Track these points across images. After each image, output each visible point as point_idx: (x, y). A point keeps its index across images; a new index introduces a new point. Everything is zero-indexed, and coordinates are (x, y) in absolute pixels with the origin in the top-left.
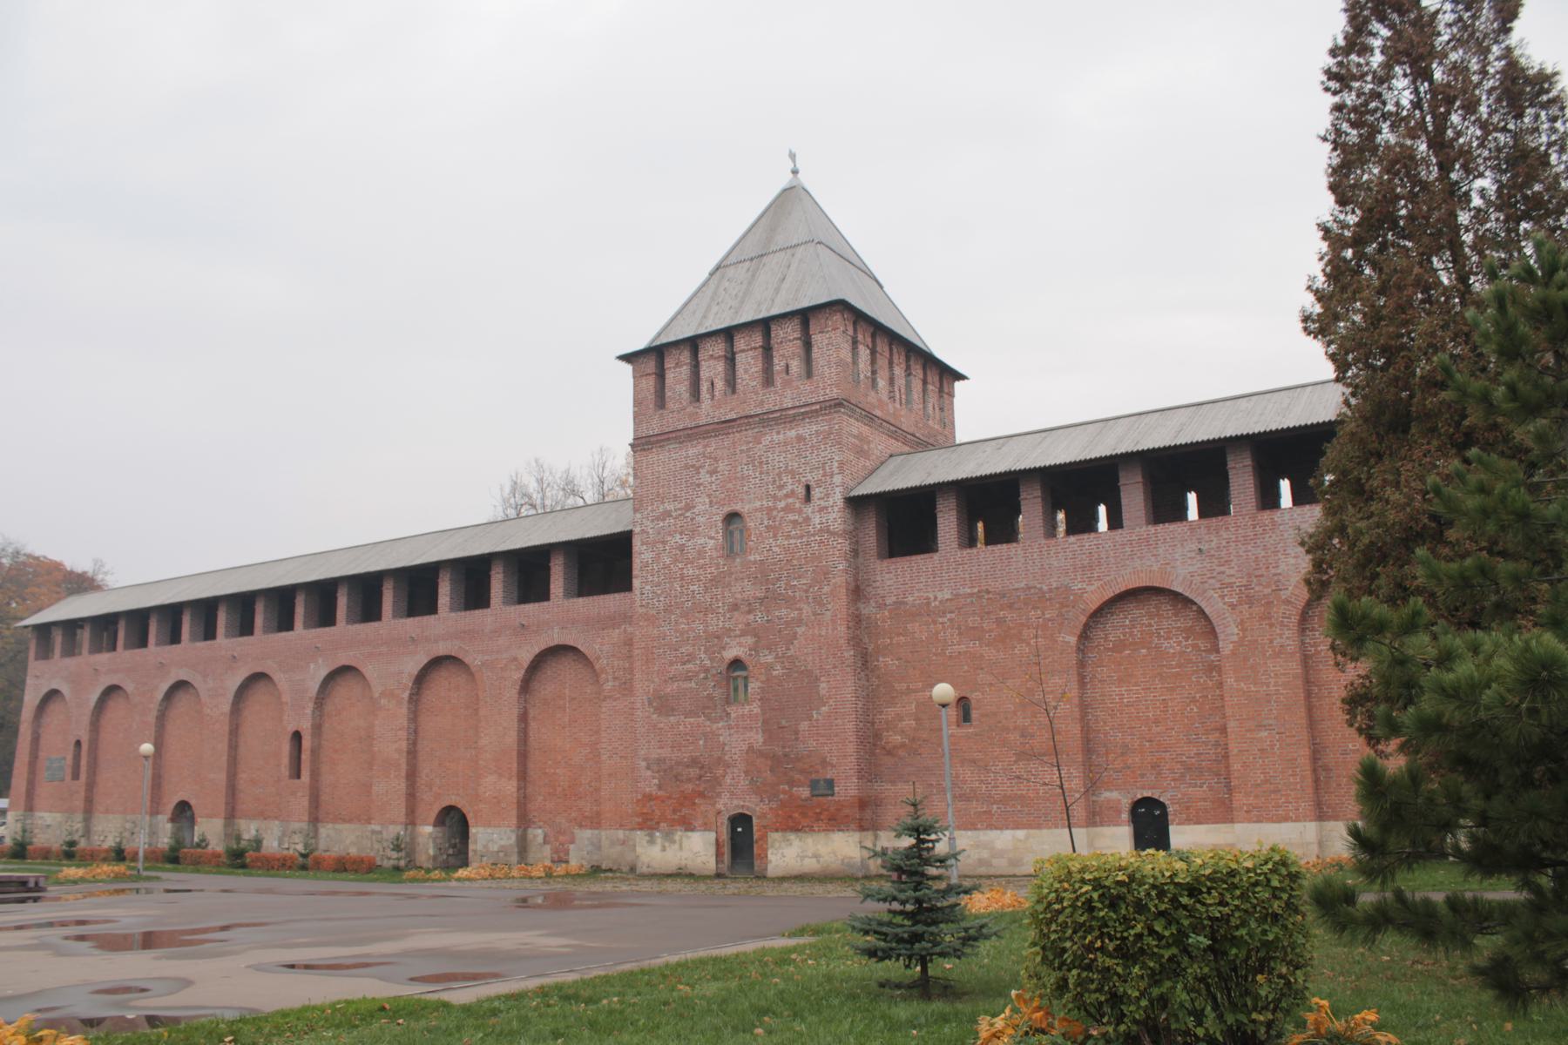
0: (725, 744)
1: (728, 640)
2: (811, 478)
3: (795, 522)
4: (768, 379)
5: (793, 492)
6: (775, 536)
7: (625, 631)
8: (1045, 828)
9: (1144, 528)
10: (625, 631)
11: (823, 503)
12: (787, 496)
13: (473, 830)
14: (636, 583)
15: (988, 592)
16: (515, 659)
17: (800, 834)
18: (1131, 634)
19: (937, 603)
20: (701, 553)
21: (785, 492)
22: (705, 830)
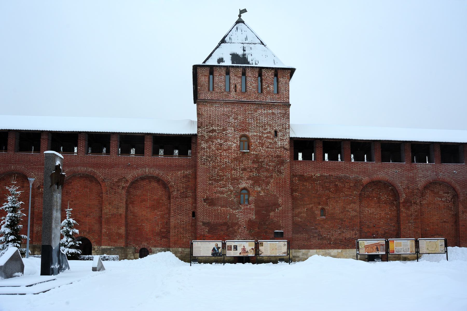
0: (239, 218)
1: (241, 181)
3: (271, 143)
5: (270, 132)
8: (347, 249)
10: (184, 172)
11: (282, 138)
12: (267, 133)
21: (267, 131)
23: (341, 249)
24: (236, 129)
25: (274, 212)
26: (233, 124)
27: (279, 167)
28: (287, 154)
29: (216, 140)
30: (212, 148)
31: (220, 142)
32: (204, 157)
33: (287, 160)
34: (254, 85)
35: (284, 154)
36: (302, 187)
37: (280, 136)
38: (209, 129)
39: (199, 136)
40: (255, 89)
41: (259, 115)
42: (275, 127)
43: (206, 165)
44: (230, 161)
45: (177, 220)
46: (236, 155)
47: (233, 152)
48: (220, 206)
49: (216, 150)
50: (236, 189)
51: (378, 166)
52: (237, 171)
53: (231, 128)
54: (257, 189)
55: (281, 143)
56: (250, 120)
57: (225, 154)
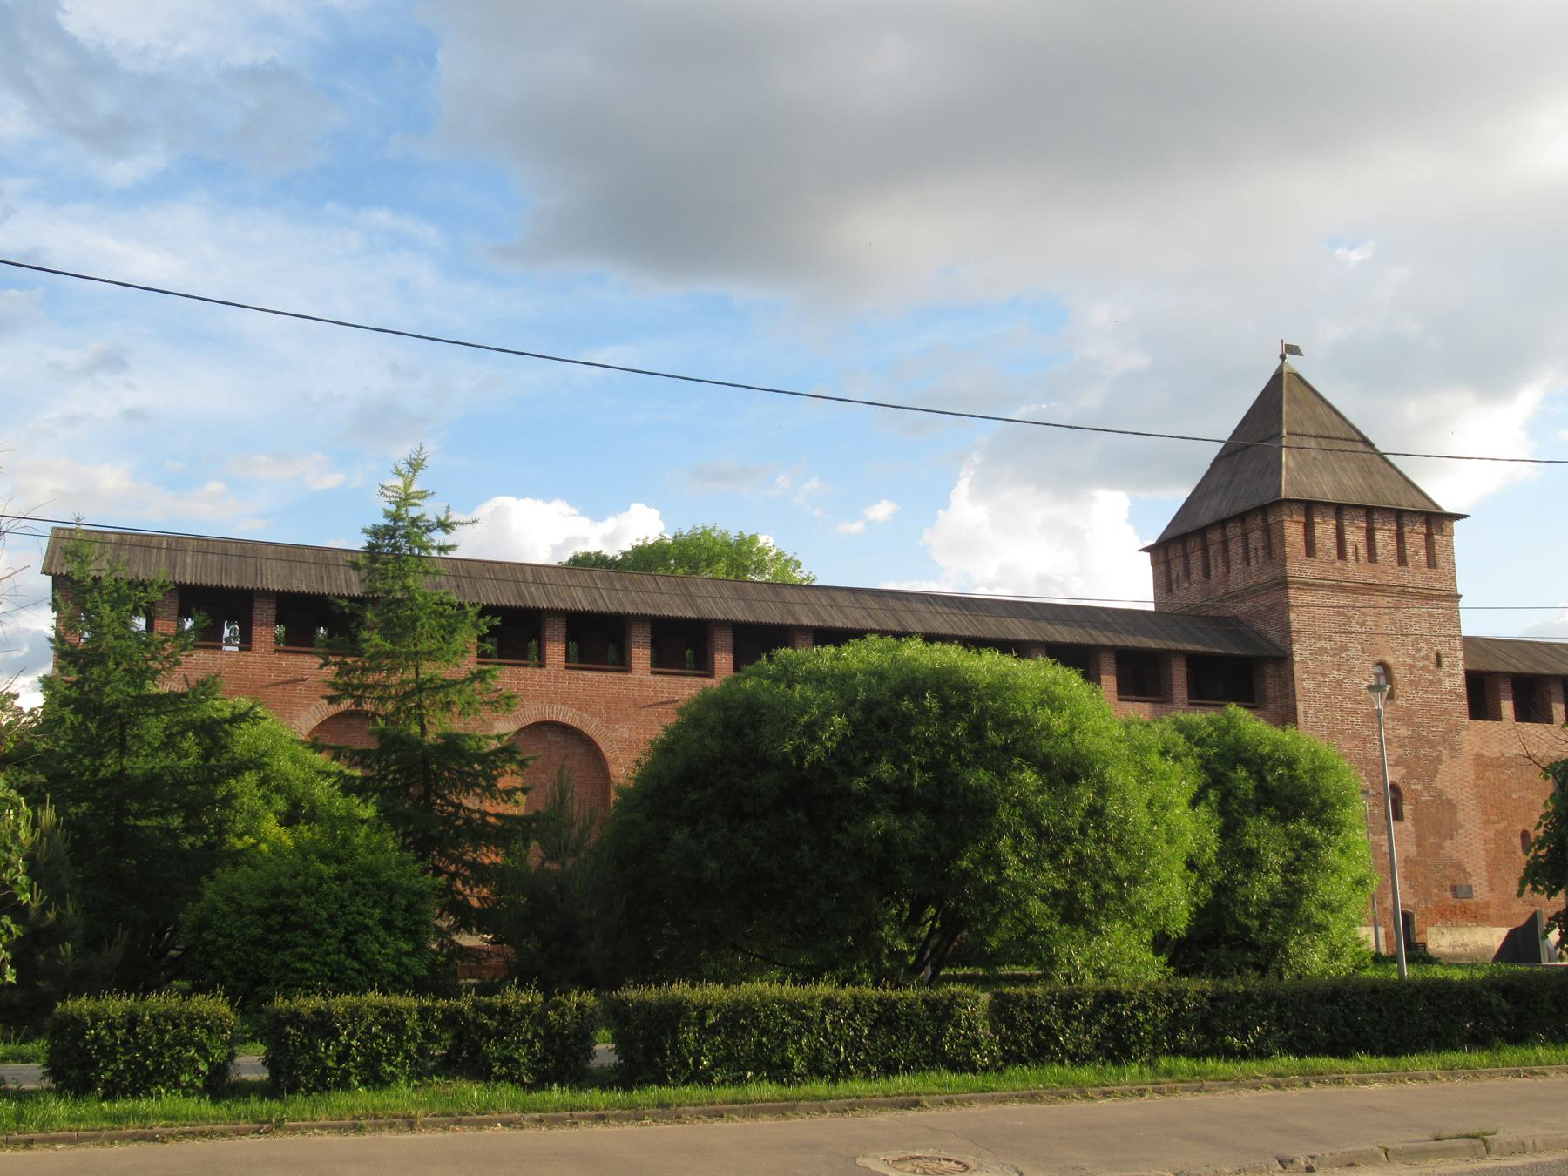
3: (1431, 682)
5: (1427, 655)
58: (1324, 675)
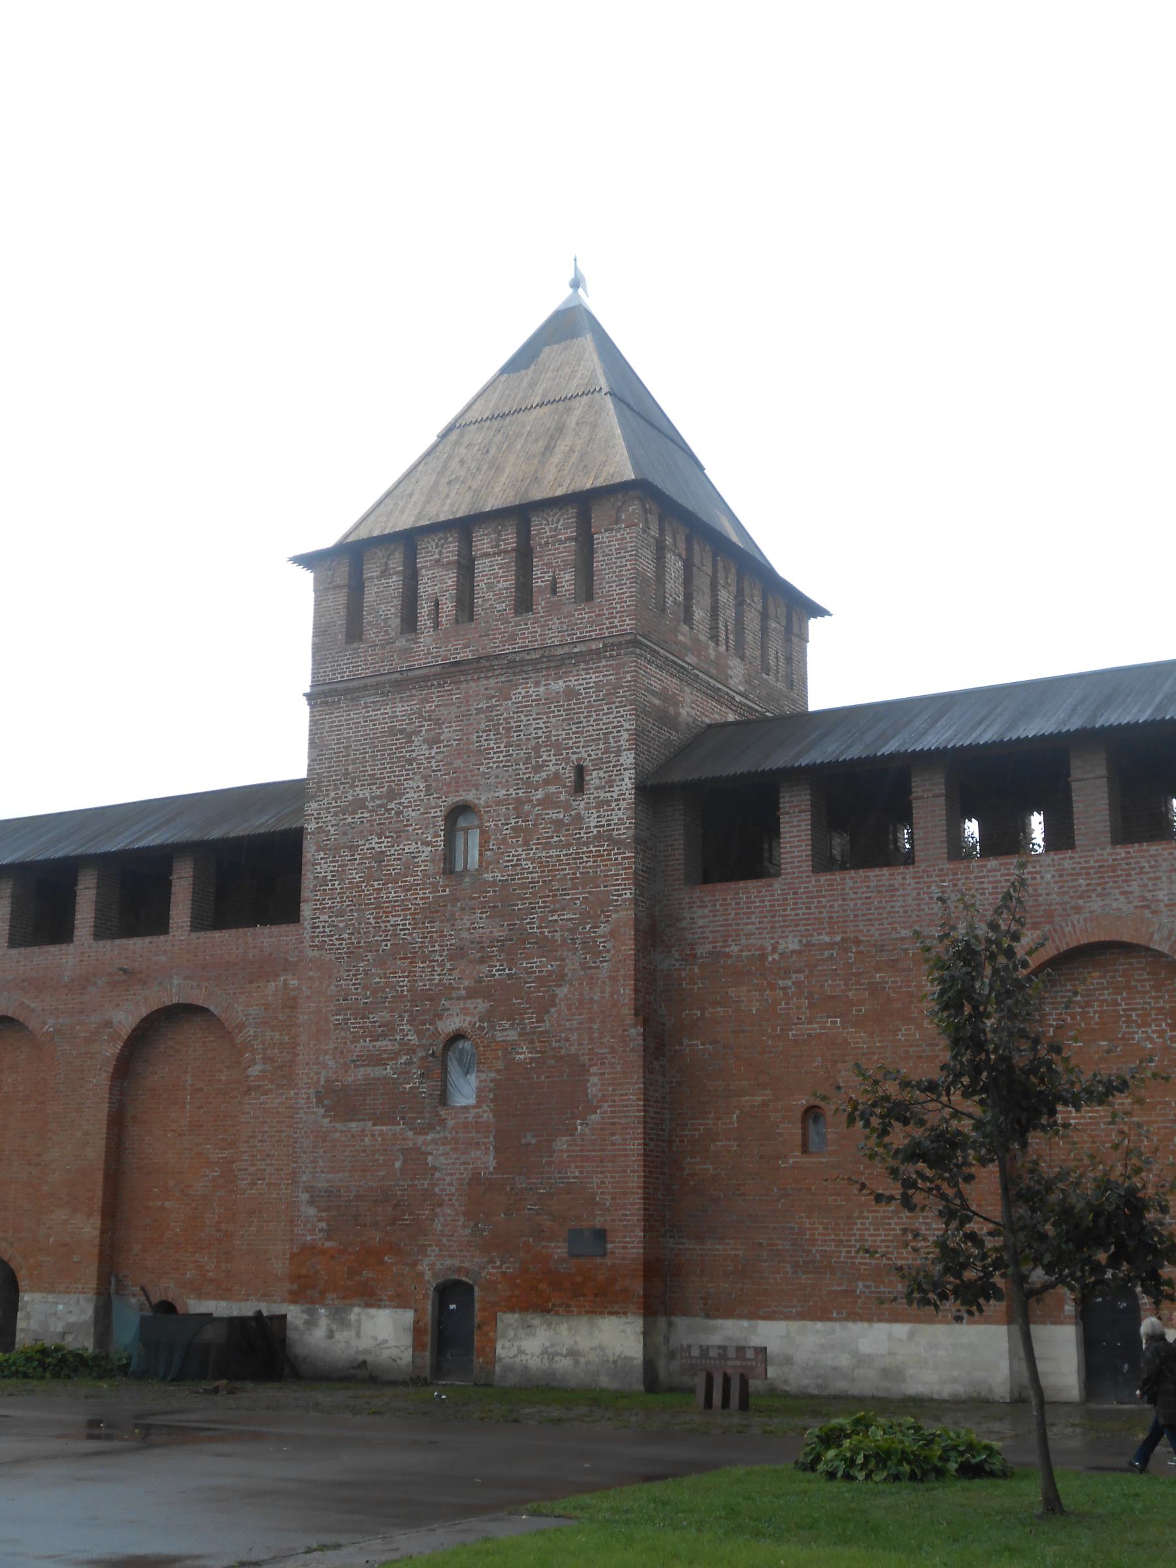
0: (435, 1168)
1: (447, 1004)
2: (586, 755)
3: (558, 823)
4: (524, 600)
5: (556, 774)
6: (526, 843)
7: (285, 983)
9: (1109, 850)
10: (285, 983)
11: (602, 794)
12: (547, 782)
13: (26, 1297)
14: (306, 910)
15: (858, 942)
16: (109, 1024)
17: (548, 1316)
18: (1084, 1014)
19: (776, 957)
20: (409, 866)
21: (544, 775)
22: (397, 1307)
23: (909, 1321)
24: (434, 785)
25: (571, 1135)
26: (422, 764)
27: (588, 926)
28: (621, 864)
29: (363, 842)
30: (351, 874)
31: (376, 846)
32: (324, 917)
33: (623, 890)
34: (500, 586)
35: (612, 865)
36: (719, 1009)
37: (596, 788)
38: (344, 799)
39: (310, 834)
40: (503, 602)
41: (518, 707)
42: (578, 750)
43: (330, 949)
44: (410, 924)
45: (257, 1184)
46: (431, 895)
47: (419, 884)
48: (369, 1119)
49: (363, 882)
50: (428, 1039)
51: (1093, 867)
52: (434, 961)
53: (415, 785)
54: (505, 1034)
55: (598, 817)
56: (485, 735)
57: (393, 895)
58: (352, 848)
